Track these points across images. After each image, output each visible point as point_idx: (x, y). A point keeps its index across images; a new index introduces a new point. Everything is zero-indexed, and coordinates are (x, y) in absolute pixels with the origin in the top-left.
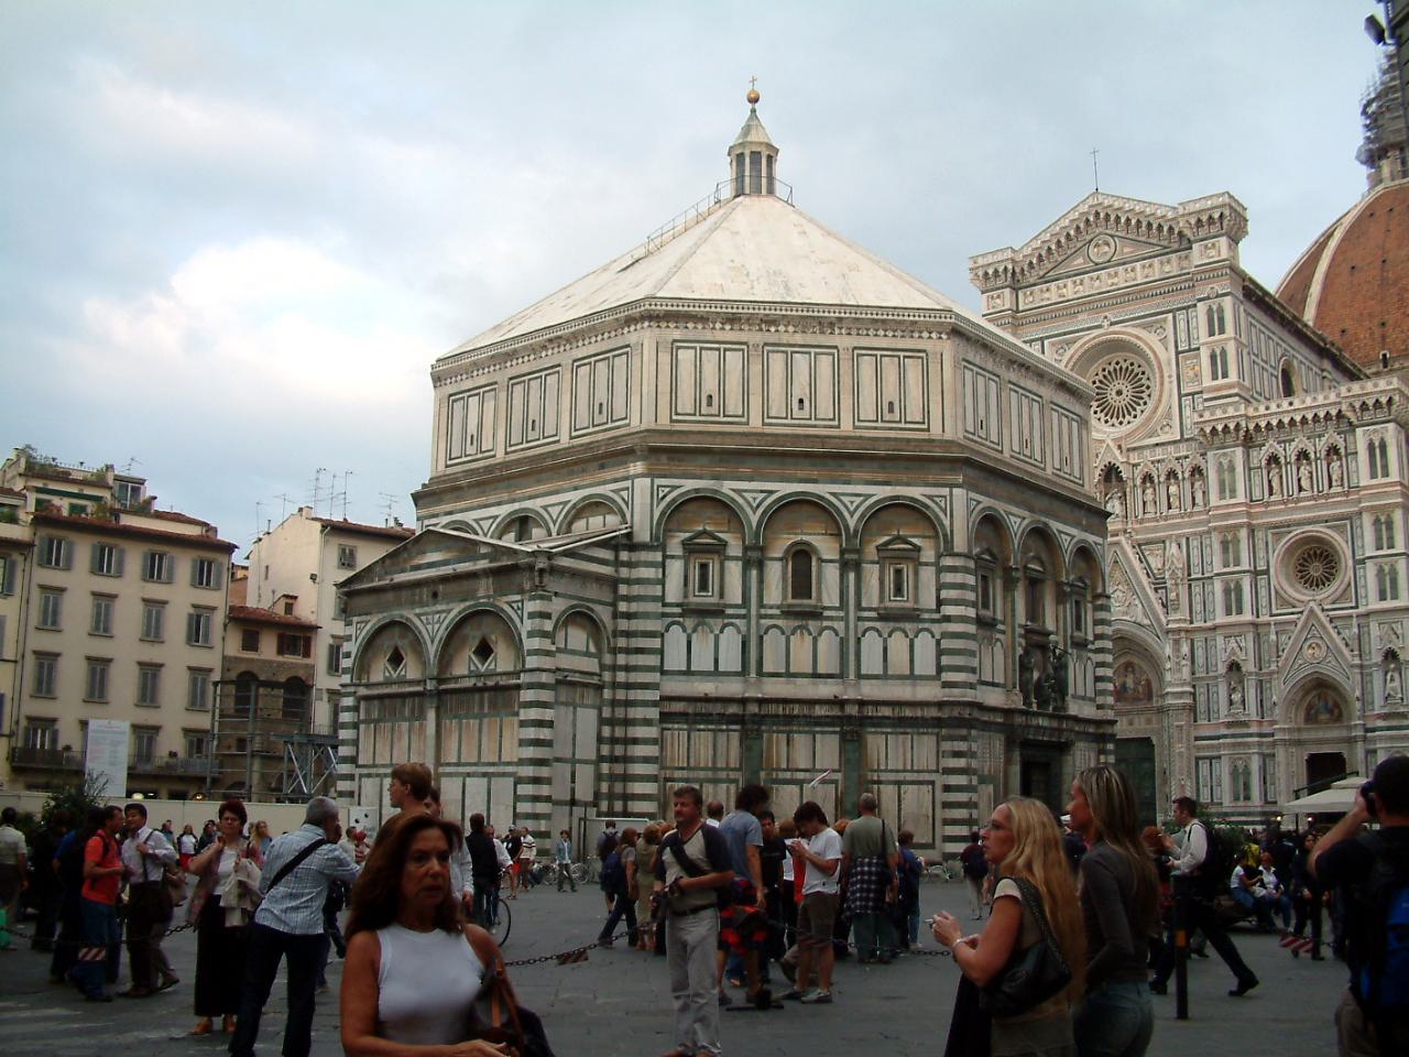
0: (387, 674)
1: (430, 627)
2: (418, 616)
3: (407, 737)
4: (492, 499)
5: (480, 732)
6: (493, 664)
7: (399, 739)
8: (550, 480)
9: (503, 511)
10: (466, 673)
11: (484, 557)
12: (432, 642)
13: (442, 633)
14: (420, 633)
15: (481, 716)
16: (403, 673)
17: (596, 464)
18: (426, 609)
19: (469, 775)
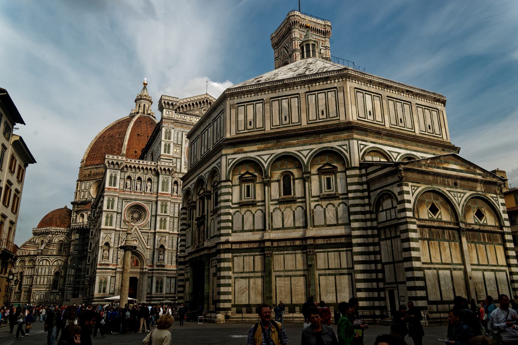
0: (430, 216)
1: (456, 198)
2: (449, 191)
3: (448, 249)
4: (396, 144)
5: (486, 250)
6: (485, 221)
7: (445, 250)
8: (421, 147)
9: (403, 152)
10: (474, 223)
11: (479, 174)
12: (459, 205)
13: (455, 201)
14: (451, 200)
15: (485, 244)
16: (440, 217)
17: (441, 149)
18: (452, 189)
19: (485, 270)
